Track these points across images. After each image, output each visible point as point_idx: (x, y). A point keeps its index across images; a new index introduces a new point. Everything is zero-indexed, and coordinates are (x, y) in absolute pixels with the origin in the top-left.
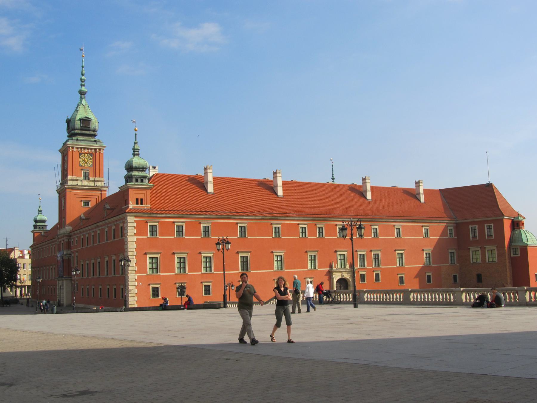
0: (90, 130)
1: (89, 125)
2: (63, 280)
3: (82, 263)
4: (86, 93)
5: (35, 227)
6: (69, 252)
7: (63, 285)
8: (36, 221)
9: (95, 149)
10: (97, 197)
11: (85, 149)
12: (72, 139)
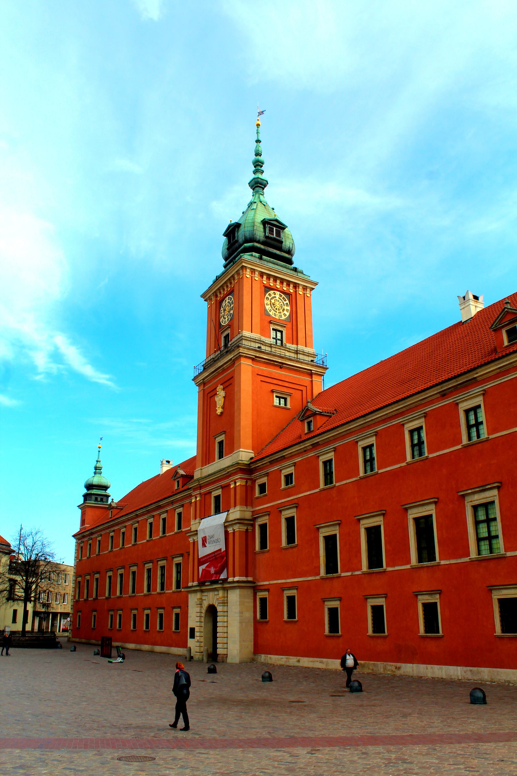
0: (280, 249)
1: (280, 236)
2: (226, 589)
3: (324, 532)
4: (265, 186)
5: (86, 497)
6: (248, 515)
7: (225, 603)
8: (89, 486)
9: (296, 285)
10: (304, 389)
11: (276, 279)
12: (252, 255)
